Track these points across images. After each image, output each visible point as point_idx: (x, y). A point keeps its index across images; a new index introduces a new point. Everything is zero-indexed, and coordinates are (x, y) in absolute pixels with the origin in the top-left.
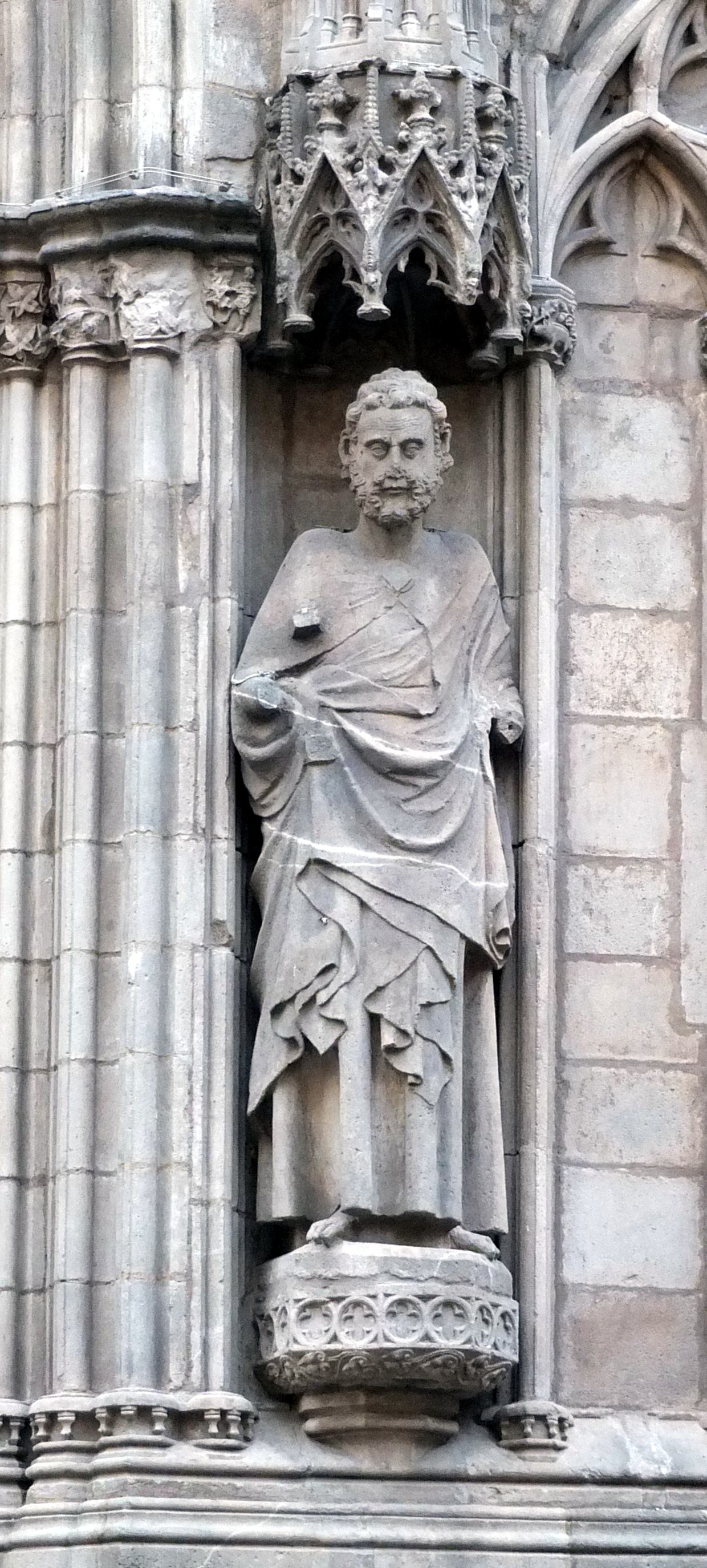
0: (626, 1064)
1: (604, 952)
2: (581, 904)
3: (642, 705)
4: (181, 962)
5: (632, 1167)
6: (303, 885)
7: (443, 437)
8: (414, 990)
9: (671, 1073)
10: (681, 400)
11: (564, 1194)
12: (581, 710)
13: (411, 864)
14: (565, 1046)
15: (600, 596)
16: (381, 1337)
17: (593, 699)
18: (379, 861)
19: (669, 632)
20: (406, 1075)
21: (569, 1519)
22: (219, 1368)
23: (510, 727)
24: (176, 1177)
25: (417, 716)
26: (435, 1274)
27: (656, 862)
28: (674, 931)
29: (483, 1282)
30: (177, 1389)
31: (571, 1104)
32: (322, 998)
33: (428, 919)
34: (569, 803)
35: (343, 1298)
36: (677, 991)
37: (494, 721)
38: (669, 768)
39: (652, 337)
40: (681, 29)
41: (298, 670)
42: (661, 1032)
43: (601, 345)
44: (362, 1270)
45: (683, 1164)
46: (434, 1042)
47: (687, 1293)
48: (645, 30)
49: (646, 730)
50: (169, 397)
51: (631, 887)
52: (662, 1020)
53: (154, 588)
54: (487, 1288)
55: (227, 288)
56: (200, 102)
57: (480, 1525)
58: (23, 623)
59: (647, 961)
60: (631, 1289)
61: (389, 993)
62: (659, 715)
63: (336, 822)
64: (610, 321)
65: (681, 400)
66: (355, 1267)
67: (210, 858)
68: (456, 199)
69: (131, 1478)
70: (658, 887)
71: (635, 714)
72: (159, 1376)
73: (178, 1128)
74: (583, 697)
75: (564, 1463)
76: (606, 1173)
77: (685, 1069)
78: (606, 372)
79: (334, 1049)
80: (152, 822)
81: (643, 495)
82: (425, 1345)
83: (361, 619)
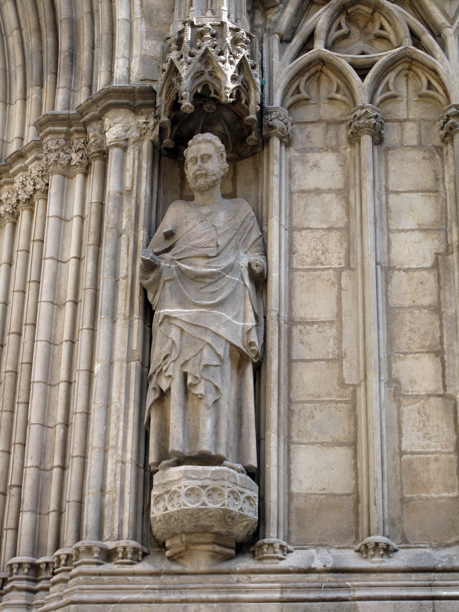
0: (318, 402)
1: (308, 358)
2: (298, 340)
3: (325, 263)
4: (116, 366)
5: (322, 443)
6: (162, 328)
7: (222, 155)
8: (201, 360)
9: (339, 405)
10: (339, 152)
11: (292, 456)
12: (298, 267)
13: (202, 312)
14: (292, 396)
15: (306, 225)
16: (182, 504)
17: (303, 262)
18: (189, 312)
19: (335, 236)
20: (197, 395)
21: (282, 588)
22: (126, 531)
23: (257, 266)
24: (110, 452)
25: (208, 257)
26: (208, 476)
27: (331, 322)
28: (340, 347)
29: (232, 480)
30: (108, 540)
31: (295, 419)
32: (164, 368)
33: (209, 332)
34: (293, 302)
35: (170, 491)
36: (341, 371)
37: (250, 265)
38: (337, 286)
39: (327, 131)
40: (335, 25)
41: (167, 250)
42: (334, 388)
43: (306, 136)
44: (176, 477)
45: (345, 441)
46: (211, 382)
47: (349, 495)
48: (317, 22)
49: (326, 272)
50: (123, 162)
51: (321, 332)
52: (335, 383)
53: (112, 228)
54: (236, 484)
55: (144, 120)
56: (138, 61)
57: (240, 592)
58: (75, 257)
59: (328, 361)
60: (322, 494)
61: (190, 362)
62: (332, 266)
63: (174, 301)
64: (310, 127)
65: (339, 152)
66: (174, 476)
67: (131, 326)
68: (221, 64)
69: (81, 578)
70: (332, 332)
71: (321, 267)
72: (100, 535)
73: (112, 432)
74: (299, 262)
75: (282, 565)
76: (310, 447)
77: (346, 402)
78: (308, 145)
79: (169, 389)
80: (107, 314)
81: (324, 187)
82: (202, 507)
83: (190, 226)
